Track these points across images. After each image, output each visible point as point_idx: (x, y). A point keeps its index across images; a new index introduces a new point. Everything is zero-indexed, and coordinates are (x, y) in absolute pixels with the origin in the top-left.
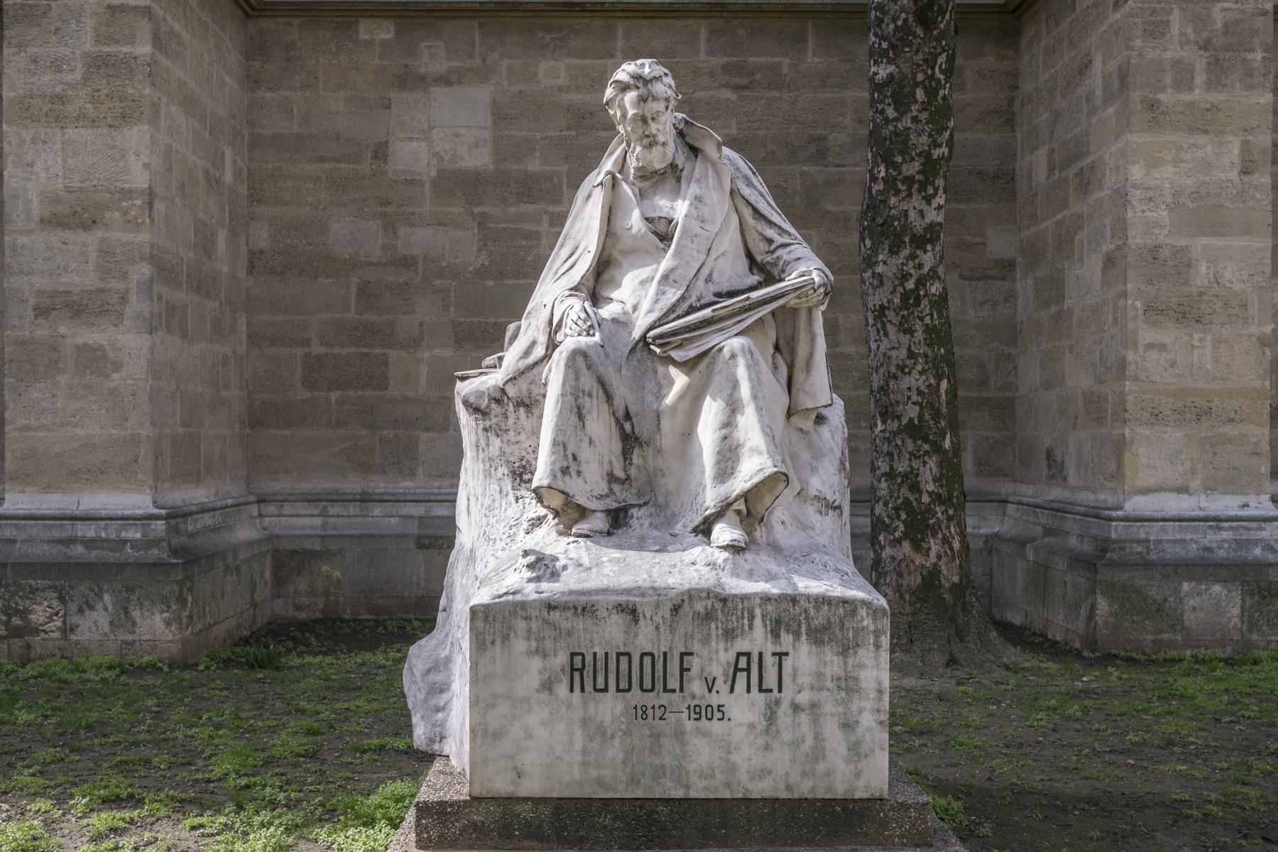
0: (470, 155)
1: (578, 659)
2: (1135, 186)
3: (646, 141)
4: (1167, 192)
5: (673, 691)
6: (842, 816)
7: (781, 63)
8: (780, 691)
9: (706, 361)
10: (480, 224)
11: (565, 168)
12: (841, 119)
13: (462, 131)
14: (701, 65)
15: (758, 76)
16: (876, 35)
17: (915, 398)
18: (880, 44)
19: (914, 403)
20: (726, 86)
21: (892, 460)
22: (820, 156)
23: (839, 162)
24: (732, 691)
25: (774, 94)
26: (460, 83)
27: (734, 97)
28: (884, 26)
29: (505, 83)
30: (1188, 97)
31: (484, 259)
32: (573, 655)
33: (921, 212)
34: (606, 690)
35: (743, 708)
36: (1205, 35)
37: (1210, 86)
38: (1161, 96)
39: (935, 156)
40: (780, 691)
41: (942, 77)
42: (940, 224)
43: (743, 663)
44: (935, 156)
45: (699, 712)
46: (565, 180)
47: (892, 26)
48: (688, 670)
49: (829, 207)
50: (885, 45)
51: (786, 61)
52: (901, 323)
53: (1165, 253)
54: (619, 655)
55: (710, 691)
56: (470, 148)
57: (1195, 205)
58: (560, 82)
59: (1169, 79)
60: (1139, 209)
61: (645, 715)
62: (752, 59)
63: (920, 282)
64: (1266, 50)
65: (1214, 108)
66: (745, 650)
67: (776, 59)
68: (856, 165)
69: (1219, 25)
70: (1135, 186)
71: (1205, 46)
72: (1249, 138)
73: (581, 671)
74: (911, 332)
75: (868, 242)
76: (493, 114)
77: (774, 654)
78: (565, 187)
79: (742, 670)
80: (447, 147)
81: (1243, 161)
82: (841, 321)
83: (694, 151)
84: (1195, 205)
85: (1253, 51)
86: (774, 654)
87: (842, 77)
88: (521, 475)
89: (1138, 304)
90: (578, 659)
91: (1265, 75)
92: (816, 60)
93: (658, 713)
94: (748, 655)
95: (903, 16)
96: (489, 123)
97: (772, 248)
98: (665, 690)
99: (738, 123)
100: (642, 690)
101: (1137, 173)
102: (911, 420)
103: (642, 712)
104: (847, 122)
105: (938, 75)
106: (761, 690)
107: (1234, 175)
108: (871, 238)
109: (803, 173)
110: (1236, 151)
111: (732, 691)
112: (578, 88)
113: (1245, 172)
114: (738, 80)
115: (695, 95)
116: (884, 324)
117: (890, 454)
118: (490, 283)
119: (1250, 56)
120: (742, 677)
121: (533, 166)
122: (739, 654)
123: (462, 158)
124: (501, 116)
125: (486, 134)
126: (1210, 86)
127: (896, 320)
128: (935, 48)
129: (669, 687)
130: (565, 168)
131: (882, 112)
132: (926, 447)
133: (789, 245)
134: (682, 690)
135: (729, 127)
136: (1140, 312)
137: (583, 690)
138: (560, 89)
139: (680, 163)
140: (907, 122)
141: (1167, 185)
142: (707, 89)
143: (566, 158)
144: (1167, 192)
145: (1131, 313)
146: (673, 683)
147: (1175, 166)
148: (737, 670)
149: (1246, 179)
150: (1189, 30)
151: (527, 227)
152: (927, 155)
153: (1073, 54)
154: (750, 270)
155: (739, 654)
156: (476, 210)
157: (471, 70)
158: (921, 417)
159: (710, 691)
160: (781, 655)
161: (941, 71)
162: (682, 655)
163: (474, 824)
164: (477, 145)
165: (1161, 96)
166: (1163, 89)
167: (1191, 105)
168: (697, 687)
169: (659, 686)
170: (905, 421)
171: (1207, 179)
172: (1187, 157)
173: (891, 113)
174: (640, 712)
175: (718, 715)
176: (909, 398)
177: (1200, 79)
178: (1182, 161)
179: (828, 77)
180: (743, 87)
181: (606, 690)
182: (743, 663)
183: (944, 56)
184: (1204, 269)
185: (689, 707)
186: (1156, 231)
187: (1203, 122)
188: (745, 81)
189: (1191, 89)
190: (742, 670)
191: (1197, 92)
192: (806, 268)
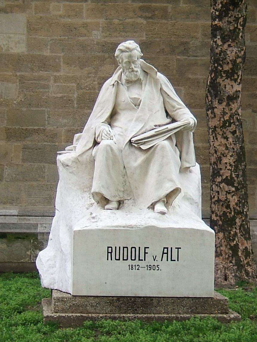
0: (16, 47)
1: (110, 249)
3: (130, 70)
5: (142, 260)
7: (168, 6)
8: (178, 260)
10: (20, 80)
11: (62, 54)
12: (196, 34)
13: (12, 35)
14: (129, 6)
15: (156, 13)
16: (214, 8)
17: (229, 167)
18: (215, 13)
19: (228, 170)
20: (141, 17)
21: (218, 194)
22: (185, 52)
24: (162, 260)
26: (12, 12)
27: (145, 22)
28: (217, 5)
29: (34, 13)
31: (21, 98)
32: (108, 247)
33: (232, 85)
34: (119, 260)
35: (165, 265)
39: (238, 62)
40: (178, 260)
41: (241, 28)
42: (239, 91)
43: (166, 251)
44: (238, 62)
45: (150, 267)
46: (62, 60)
47: (220, 5)
48: (147, 253)
50: (217, 13)
51: (170, 6)
52: (223, 134)
55: (154, 260)
56: (16, 44)
58: (61, 13)
61: (132, 269)
62: (154, 4)
63: (231, 116)
67: (165, 5)
68: (203, 56)
73: (111, 253)
74: (227, 138)
75: (210, 98)
76: (27, 28)
77: (176, 248)
78: (62, 64)
79: (165, 253)
80: (4, 43)
83: (146, 73)
86: (176, 248)
87: (197, 14)
88: (83, 189)
90: (110, 249)
92: (184, 6)
93: (137, 267)
94: (167, 248)
96: (25, 32)
97: (174, 110)
98: (139, 260)
99: (146, 35)
100: (132, 260)
102: (227, 177)
103: (132, 267)
104: (199, 35)
105: (239, 27)
106: (171, 260)
108: (211, 96)
109: (178, 60)
111: (162, 260)
112: (69, 16)
114: (147, 14)
115: (126, 21)
116: (216, 134)
117: (218, 192)
118: (24, 109)
120: (165, 255)
121: (47, 53)
122: (164, 248)
123: (11, 48)
124: (31, 28)
125: (24, 37)
127: (221, 133)
128: (238, 15)
129: (140, 259)
130: (62, 54)
131: (216, 42)
132: (233, 189)
133: (181, 108)
134: (145, 260)
137: (111, 259)
138: (60, 16)
139: (142, 78)
140: (226, 46)
142: (131, 18)
143: (63, 50)
146: (142, 257)
148: (163, 253)
151: (43, 82)
154: (167, 117)
155: (164, 248)
156: (18, 74)
157: (17, 6)
158: (231, 175)
159: (154, 260)
161: (241, 25)
162: (145, 248)
164: (19, 42)
168: (149, 258)
170: (224, 177)
173: (219, 43)
174: (130, 267)
176: (226, 167)
179: (190, 14)
182: (166, 251)
183: (242, 18)
188: (150, 15)
190: (165, 253)
192: (187, 117)
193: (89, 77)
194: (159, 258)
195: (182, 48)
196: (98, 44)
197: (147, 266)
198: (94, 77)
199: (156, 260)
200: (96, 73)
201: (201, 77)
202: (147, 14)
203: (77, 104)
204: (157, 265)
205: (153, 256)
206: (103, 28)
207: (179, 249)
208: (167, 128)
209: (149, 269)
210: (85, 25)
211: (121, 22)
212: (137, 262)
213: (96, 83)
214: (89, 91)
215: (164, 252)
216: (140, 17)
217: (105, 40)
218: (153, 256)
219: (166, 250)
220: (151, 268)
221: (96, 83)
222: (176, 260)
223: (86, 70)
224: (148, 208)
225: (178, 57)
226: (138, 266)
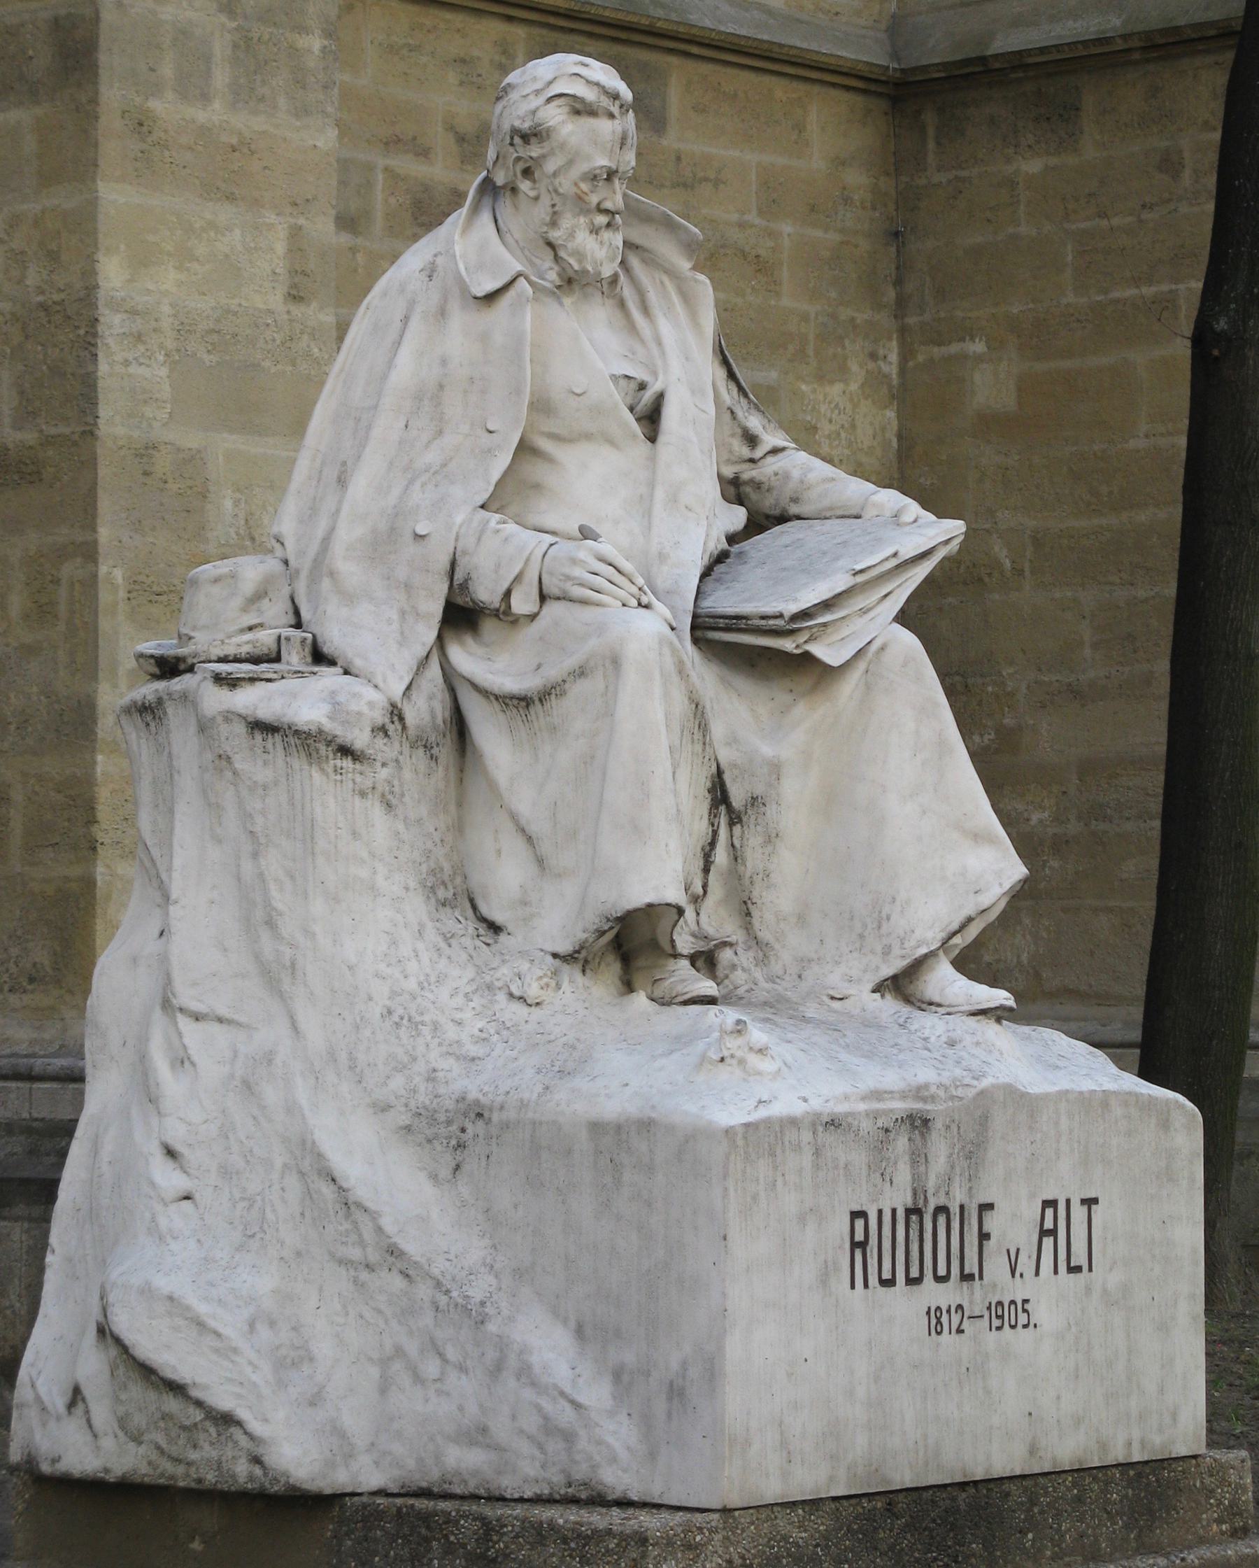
2: (116, 306)
4: (166, 323)
6: (1145, 1491)
8: (1090, 1270)
9: (862, 666)
24: (1037, 1274)
32: (855, 1215)
34: (890, 1283)
38: (155, 105)
40: (1090, 1270)
53: (163, 463)
54: (909, 1212)
57: (214, 358)
59: (167, 70)
60: (118, 358)
64: (328, 34)
65: (243, 147)
66: (1050, 1197)
70: (116, 306)
72: (301, 221)
73: (863, 1245)
77: (1083, 1201)
81: (293, 272)
84: (214, 358)
85: (302, 29)
86: (1083, 1201)
89: (118, 575)
91: (325, 87)
101: (112, 273)
107: (276, 300)
110: (280, 248)
111: (1037, 1274)
113: (295, 297)
119: (303, 42)
126: (243, 95)
129: (967, 1271)
134: (981, 1278)
136: (122, 594)
137: (866, 1286)
141: (166, 309)
144: (166, 323)
145: (104, 597)
147: (179, 268)
148: (1043, 1233)
149: (297, 310)
160: (1090, 1202)
168: (996, 1267)
172: (201, 250)
177: (221, 77)
184: (228, 504)
185: (989, 1308)
186: (148, 411)
187: (229, 174)
189: (205, 98)
191: (217, 105)
197: (989, 1308)
199: (1017, 1274)
204: (1025, 1301)
205: (1008, 1251)
207: (1094, 1207)
208: (895, 555)
209: (996, 1323)
215: (1045, 1228)
218: (1008, 1251)
219: (1049, 1212)
220: (1001, 1317)
222: (1085, 1268)
224: (874, 991)
226: (960, 1312)
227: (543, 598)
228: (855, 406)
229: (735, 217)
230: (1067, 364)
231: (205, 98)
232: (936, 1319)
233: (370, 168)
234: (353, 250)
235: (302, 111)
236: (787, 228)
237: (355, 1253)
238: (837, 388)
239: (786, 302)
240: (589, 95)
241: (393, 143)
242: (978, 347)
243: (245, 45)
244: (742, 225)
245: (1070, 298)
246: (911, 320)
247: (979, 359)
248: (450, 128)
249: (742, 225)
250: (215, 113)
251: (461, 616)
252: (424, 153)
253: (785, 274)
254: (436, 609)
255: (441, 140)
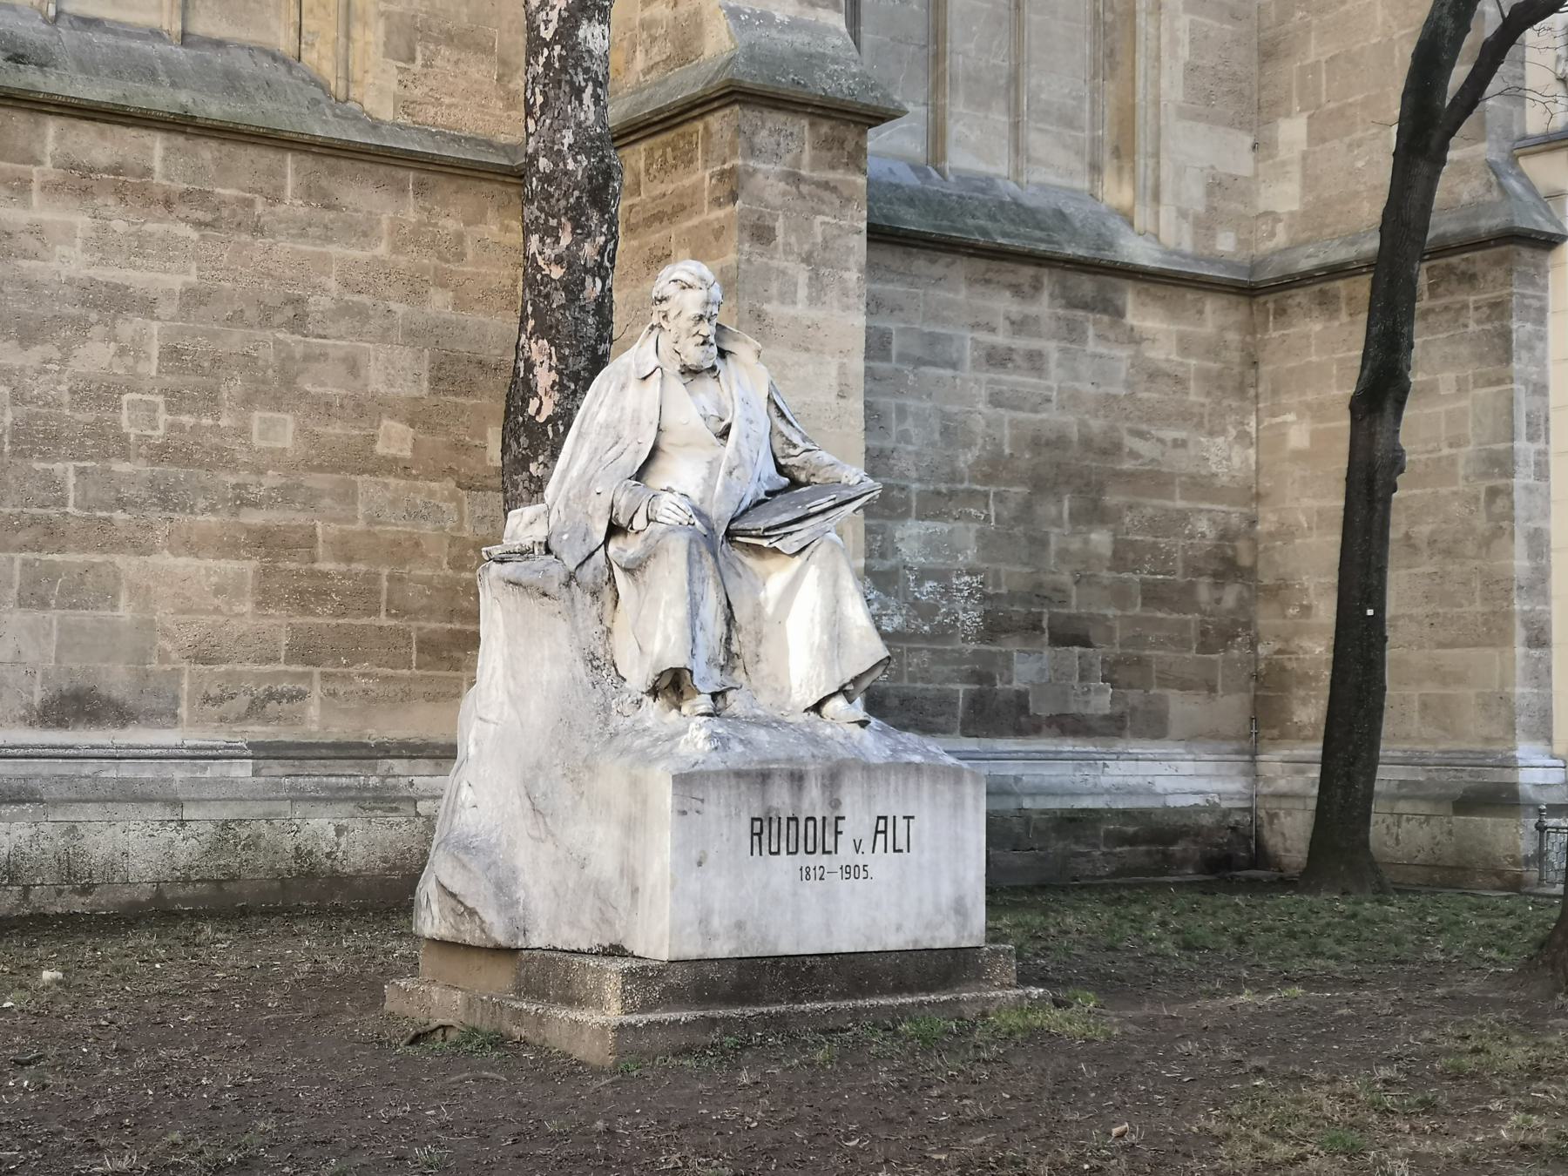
12: (323, 279)
15: (225, 213)
16: (541, 209)
18: (546, 221)
20: (186, 220)
22: (298, 323)
23: (321, 332)
25: (246, 238)
27: (195, 235)
28: (553, 201)
30: (789, 311)
32: (753, 819)
34: (778, 853)
35: (881, 864)
36: (806, 247)
37: (813, 300)
38: (765, 307)
43: (881, 828)
49: (308, 387)
68: (341, 338)
69: (819, 239)
71: (807, 259)
73: (759, 835)
81: (840, 384)
82: (319, 531)
85: (848, 269)
87: (326, 227)
93: (819, 873)
94: (885, 818)
95: (576, 193)
98: (824, 852)
99: (199, 269)
103: (806, 873)
104: (332, 284)
107: (832, 398)
109: (277, 342)
110: (834, 373)
114: (200, 215)
119: (846, 275)
120: (881, 837)
131: (547, 296)
135: (186, 272)
148: (877, 832)
149: (842, 402)
150: (793, 240)
152: (594, 349)
153: (635, 243)
163: (670, 986)
165: (765, 307)
166: (768, 300)
167: (795, 319)
169: (820, 849)
171: (808, 400)
175: (863, 874)
178: (787, 379)
179: (310, 225)
180: (207, 225)
181: (778, 853)
182: (881, 828)
188: (209, 217)
191: (800, 306)
193: (46, 372)
194: (866, 846)
195: (289, 312)
196: (70, 282)
198: (59, 372)
200: (64, 361)
201: (335, 391)
202: (200, 215)
203: (11, 443)
206: (86, 240)
210: (37, 230)
211: (134, 229)
212: (818, 859)
213: (63, 388)
214: (45, 411)
216: (182, 220)
217: (92, 272)
219: (882, 822)
221: (63, 388)
223: (35, 354)
225: (280, 336)
227: (649, 521)
228: (1231, 448)
229: (1163, 357)
230: (1332, 425)
231: (794, 303)
232: (806, 873)
233: (962, 338)
234: (954, 378)
235: (847, 308)
236: (1193, 362)
237: (535, 833)
238: (1220, 440)
239: (1192, 398)
240: (689, 280)
241: (975, 326)
242: (1291, 417)
243: (815, 278)
244: (1167, 360)
245: (1335, 392)
246: (1261, 405)
247: (1293, 423)
248: (1008, 318)
249: (1167, 360)
250: (801, 309)
251: (614, 530)
252: (993, 330)
253: (1192, 384)
254: (603, 527)
255: (1001, 323)
